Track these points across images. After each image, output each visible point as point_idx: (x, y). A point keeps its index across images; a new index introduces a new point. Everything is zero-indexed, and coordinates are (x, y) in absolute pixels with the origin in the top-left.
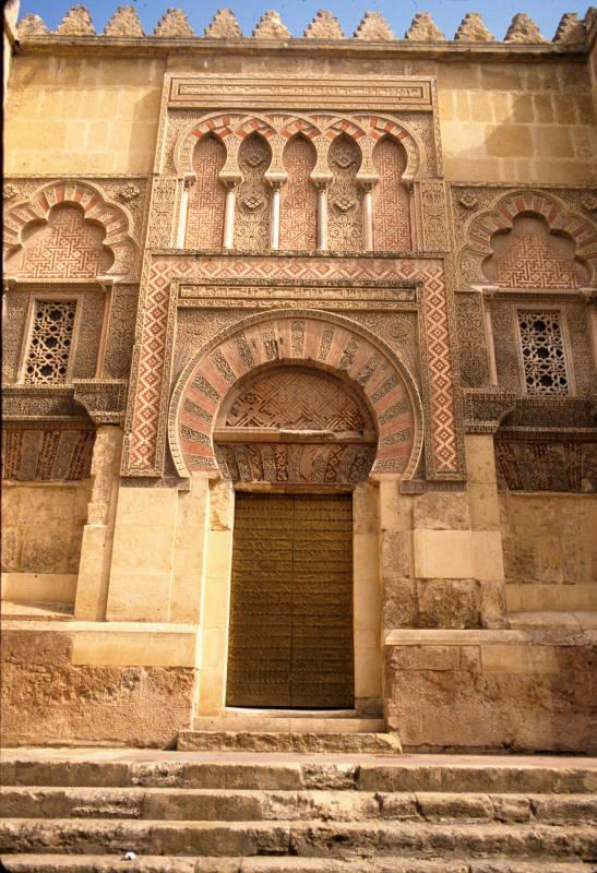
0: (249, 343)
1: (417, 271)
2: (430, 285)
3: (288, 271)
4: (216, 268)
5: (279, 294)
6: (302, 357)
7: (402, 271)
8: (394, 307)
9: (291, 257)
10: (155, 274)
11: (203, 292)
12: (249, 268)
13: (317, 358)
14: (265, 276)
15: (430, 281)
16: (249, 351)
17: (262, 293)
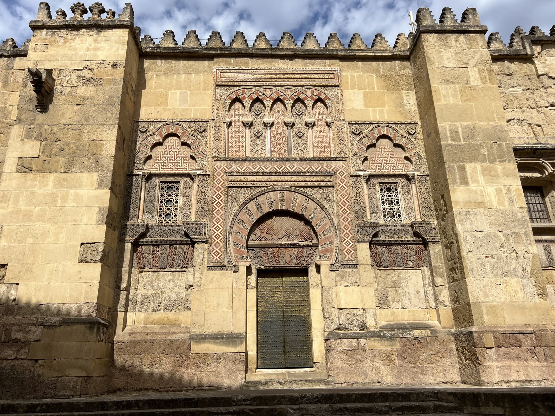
0: (261, 203)
1: (333, 167)
2: (339, 173)
3: (276, 168)
4: (244, 167)
5: (273, 179)
6: (284, 208)
7: (327, 167)
8: (324, 184)
9: (277, 161)
10: (217, 170)
11: (239, 178)
12: (259, 167)
13: (291, 209)
14: (266, 171)
15: (339, 171)
16: (261, 207)
17: (266, 179)
